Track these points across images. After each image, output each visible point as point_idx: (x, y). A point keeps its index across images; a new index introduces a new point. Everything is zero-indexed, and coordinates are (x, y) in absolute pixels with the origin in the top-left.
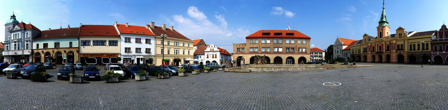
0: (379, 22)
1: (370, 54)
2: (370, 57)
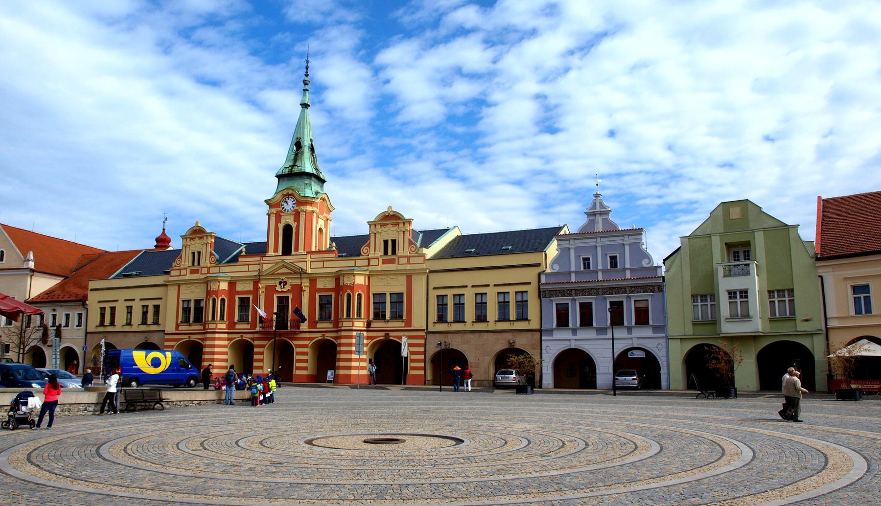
0: (279, 177)
1: (226, 336)
2: (225, 353)
